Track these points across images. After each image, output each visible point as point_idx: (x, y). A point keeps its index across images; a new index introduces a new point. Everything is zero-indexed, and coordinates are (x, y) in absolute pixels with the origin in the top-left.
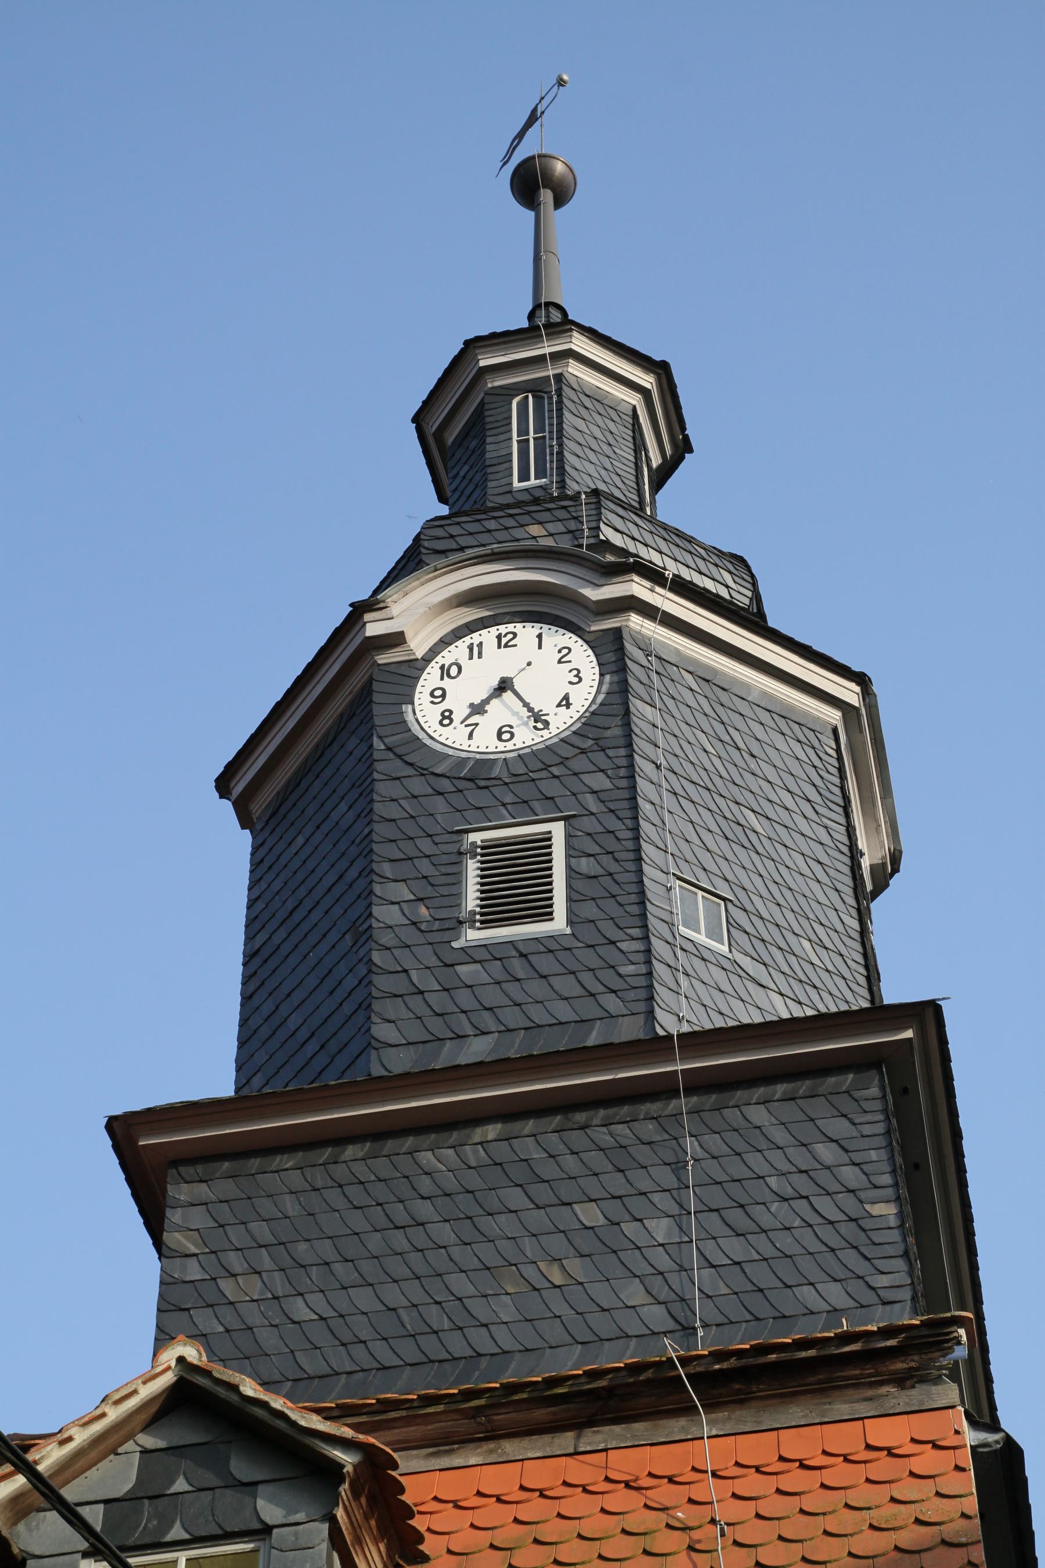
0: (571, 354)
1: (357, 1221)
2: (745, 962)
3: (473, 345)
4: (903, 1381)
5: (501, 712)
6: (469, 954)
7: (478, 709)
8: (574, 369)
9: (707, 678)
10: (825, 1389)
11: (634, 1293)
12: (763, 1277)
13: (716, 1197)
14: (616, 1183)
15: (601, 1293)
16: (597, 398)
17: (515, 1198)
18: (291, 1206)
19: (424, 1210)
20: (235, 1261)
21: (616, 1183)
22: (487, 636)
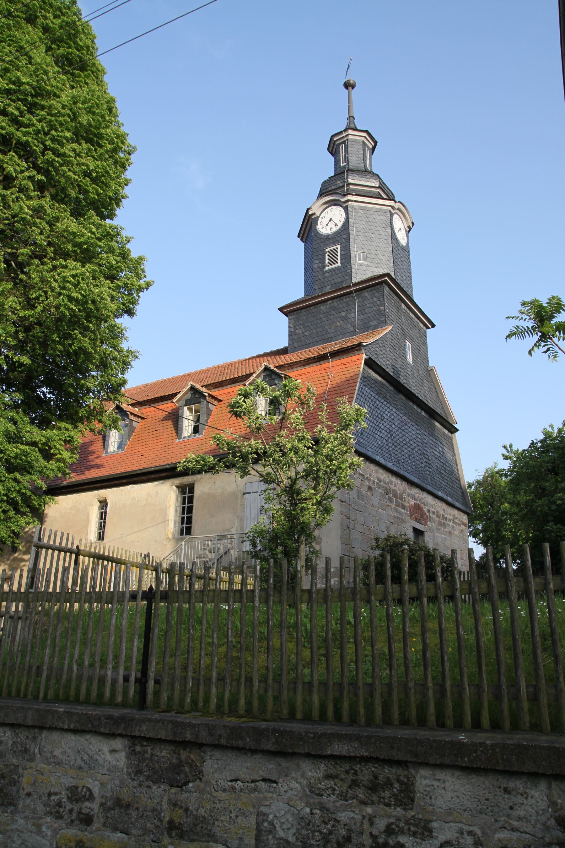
0: (348, 135)
1: (313, 319)
2: (369, 264)
3: (332, 137)
4: (357, 350)
5: (331, 225)
6: (327, 272)
7: (327, 225)
8: (350, 137)
9: (364, 209)
10: (348, 353)
11: (349, 326)
12: (366, 321)
13: (360, 309)
14: (347, 308)
15: (345, 326)
16: (356, 141)
17: (334, 312)
18: (304, 317)
19: (322, 316)
20: (298, 327)
21: (347, 308)
22: (328, 210)
